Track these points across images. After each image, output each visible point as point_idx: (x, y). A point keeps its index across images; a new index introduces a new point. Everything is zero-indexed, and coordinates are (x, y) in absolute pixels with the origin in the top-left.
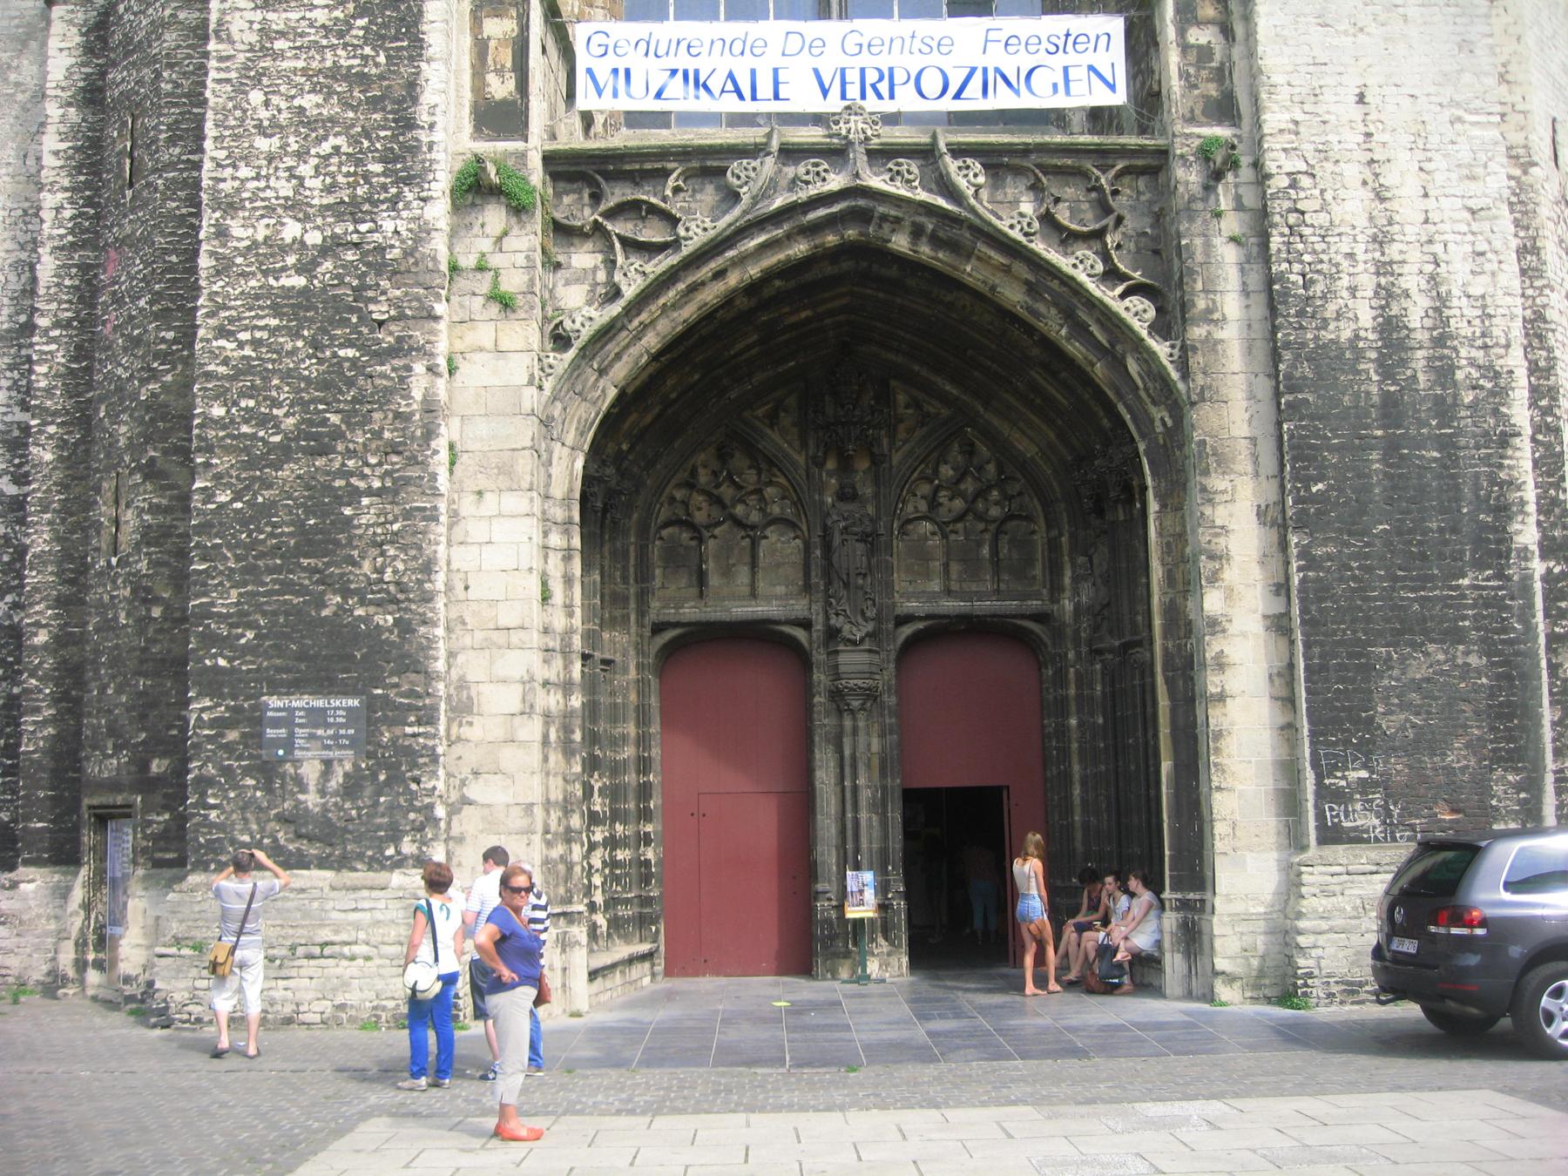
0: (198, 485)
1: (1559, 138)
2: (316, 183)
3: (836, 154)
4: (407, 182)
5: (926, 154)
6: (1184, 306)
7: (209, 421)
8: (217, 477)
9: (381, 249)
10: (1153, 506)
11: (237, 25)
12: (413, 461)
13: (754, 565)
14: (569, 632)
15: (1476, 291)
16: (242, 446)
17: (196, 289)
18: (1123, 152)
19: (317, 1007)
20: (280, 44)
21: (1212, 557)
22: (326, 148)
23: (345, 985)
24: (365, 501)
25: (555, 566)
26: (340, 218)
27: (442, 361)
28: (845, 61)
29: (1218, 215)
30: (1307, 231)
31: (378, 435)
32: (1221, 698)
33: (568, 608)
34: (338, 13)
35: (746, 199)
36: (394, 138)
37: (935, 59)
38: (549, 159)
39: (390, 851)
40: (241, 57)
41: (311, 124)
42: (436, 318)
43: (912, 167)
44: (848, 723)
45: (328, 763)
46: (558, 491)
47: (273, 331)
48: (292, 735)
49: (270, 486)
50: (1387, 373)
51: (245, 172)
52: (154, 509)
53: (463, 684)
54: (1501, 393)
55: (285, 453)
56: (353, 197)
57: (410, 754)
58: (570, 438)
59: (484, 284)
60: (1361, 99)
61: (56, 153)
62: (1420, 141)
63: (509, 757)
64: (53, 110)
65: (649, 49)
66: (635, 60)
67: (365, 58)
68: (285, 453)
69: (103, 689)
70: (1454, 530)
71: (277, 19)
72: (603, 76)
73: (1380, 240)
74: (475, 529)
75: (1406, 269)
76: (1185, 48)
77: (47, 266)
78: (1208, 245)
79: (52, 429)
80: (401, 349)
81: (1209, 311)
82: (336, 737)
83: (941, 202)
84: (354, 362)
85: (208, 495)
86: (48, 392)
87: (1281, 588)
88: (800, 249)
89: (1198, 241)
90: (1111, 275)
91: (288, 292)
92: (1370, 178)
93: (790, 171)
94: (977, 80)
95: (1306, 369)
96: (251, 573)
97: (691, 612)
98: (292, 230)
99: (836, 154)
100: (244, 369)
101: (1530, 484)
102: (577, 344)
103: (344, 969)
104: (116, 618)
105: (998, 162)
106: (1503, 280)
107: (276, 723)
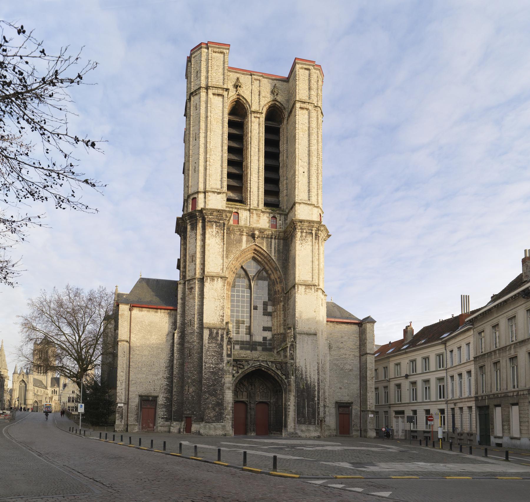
5: (266, 361)
7: (204, 383)
11: (206, 345)
17: (203, 370)
41: (213, 356)
54: (315, 387)
55: (211, 386)
57: (222, 413)
68: (211, 386)
69: (187, 405)
71: (210, 345)
73: (306, 373)
74: (227, 394)
80: (221, 377)
85: (204, 389)
87: (295, 402)
88: (254, 369)
98: (212, 366)
100: (207, 378)
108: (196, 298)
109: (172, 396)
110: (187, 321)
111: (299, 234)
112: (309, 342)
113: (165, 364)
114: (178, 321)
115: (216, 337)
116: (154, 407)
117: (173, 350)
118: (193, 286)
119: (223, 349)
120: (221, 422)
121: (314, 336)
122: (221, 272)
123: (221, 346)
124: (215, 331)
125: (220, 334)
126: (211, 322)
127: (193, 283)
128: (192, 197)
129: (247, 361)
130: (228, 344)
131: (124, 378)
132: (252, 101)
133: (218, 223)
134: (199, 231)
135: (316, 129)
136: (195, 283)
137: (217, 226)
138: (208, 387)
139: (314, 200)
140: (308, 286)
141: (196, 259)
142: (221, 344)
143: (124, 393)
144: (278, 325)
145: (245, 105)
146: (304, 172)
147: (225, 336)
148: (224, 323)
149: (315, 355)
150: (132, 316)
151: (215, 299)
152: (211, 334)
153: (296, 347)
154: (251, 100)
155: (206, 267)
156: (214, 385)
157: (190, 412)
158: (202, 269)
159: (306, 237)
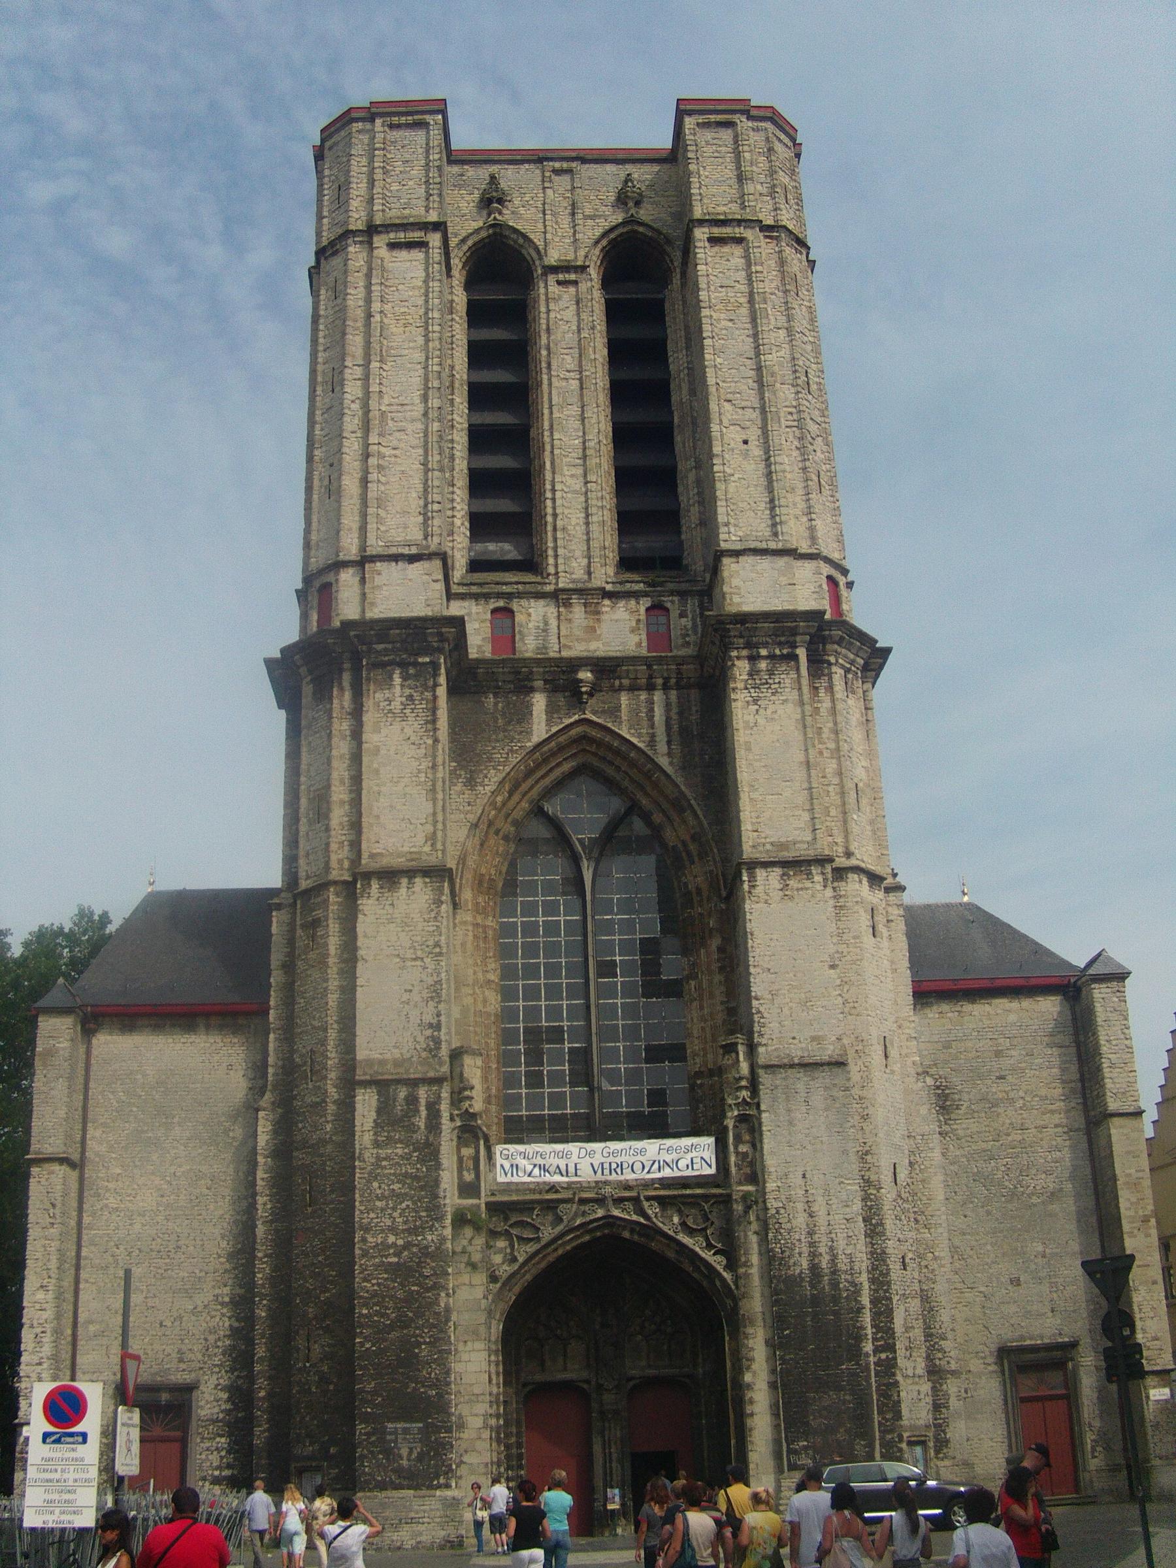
0: (358, 1340)
1: (897, 1171)
2: (400, 1220)
4: (436, 1219)
5: (636, 1200)
6: (737, 1260)
7: (361, 1315)
8: (365, 1337)
9: (427, 1247)
10: (727, 1338)
11: (367, 1155)
12: (441, 1331)
13: (565, 1356)
14: (498, 1394)
15: (848, 1252)
17: (355, 1263)
18: (714, 1196)
19: (410, 1543)
20: (384, 1163)
21: (748, 1360)
22: (404, 1205)
23: (421, 1534)
24: (423, 1347)
25: (493, 1369)
26: (410, 1234)
27: (451, 1291)
28: (603, 1160)
29: (750, 1223)
30: (782, 1231)
31: (427, 1321)
32: (752, 1415)
33: (498, 1385)
34: (406, 1150)
35: (565, 1221)
36: (429, 1202)
37: (639, 1158)
38: (487, 1204)
39: (435, 1482)
40: (369, 1168)
41: (398, 1196)
42: (449, 1274)
43: (629, 1205)
44: (607, 1425)
45: (411, 1449)
46: (493, 1339)
47: (386, 1279)
48: (397, 1438)
49: (386, 1341)
50: (813, 1286)
51: (372, 1215)
52: (329, 1345)
53: (460, 1417)
54: (857, 1292)
55: (391, 1328)
56: (415, 1226)
58: (497, 1317)
59: (465, 1259)
60: (804, 1176)
61: (263, 1179)
62: (827, 1192)
63: (479, 1445)
64: (261, 1159)
65: (525, 1156)
66: (523, 1163)
67: (417, 1169)
68: (391, 1328)
70: (840, 1347)
71: (383, 1153)
72: (507, 1166)
73: (811, 1233)
74: (465, 1357)
75: (821, 1244)
76: (737, 1153)
77: (260, 1230)
78: (746, 1236)
79: (265, 1302)
80: (436, 1287)
81: (746, 1262)
82: (414, 1438)
83: (642, 1220)
84: (418, 1292)
86: (263, 1285)
87: (773, 1371)
88: (587, 1238)
89: (742, 1234)
90: (709, 1246)
91: (390, 1264)
92: (806, 1207)
93: (582, 1208)
94: (656, 1165)
95: (782, 1286)
97: (538, 1378)
98: (391, 1239)
99: (600, 1201)
100: (375, 1294)
101: (869, 1327)
102: (501, 1281)
103: (421, 1528)
104: (310, 1388)
105: (663, 1202)
106: (858, 1247)
107: (391, 1434)
108: (331, 961)
109: (251, 1378)
110: (302, 1056)
111: (741, 669)
112: (818, 1099)
113: (224, 1244)
115: (406, 1115)
116: (178, 1434)
118: (319, 913)
119: (438, 1166)
120: (439, 1487)
121: (835, 1070)
122: (427, 849)
123: (429, 1153)
124: (402, 1093)
125: (423, 1102)
126: (388, 1056)
129: (550, 1206)
130: (461, 1142)
131: (49, 1314)
132: (549, 236)
134: (342, 700)
136: (327, 901)
139: (794, 533)
140: (795, 866)
141: (329, 810)
142: (428, 1144)
145: (524, 252)
146: (746, 442)
147: (444, 1107)
148: (444, 1052)
149: (845, 1152)
151: (404, 960)
153: (760, 1124)
154: (545, 233)
155: (364, 837)
156: (402, 1323)
157: (316, 1446)
159: (771, 673)
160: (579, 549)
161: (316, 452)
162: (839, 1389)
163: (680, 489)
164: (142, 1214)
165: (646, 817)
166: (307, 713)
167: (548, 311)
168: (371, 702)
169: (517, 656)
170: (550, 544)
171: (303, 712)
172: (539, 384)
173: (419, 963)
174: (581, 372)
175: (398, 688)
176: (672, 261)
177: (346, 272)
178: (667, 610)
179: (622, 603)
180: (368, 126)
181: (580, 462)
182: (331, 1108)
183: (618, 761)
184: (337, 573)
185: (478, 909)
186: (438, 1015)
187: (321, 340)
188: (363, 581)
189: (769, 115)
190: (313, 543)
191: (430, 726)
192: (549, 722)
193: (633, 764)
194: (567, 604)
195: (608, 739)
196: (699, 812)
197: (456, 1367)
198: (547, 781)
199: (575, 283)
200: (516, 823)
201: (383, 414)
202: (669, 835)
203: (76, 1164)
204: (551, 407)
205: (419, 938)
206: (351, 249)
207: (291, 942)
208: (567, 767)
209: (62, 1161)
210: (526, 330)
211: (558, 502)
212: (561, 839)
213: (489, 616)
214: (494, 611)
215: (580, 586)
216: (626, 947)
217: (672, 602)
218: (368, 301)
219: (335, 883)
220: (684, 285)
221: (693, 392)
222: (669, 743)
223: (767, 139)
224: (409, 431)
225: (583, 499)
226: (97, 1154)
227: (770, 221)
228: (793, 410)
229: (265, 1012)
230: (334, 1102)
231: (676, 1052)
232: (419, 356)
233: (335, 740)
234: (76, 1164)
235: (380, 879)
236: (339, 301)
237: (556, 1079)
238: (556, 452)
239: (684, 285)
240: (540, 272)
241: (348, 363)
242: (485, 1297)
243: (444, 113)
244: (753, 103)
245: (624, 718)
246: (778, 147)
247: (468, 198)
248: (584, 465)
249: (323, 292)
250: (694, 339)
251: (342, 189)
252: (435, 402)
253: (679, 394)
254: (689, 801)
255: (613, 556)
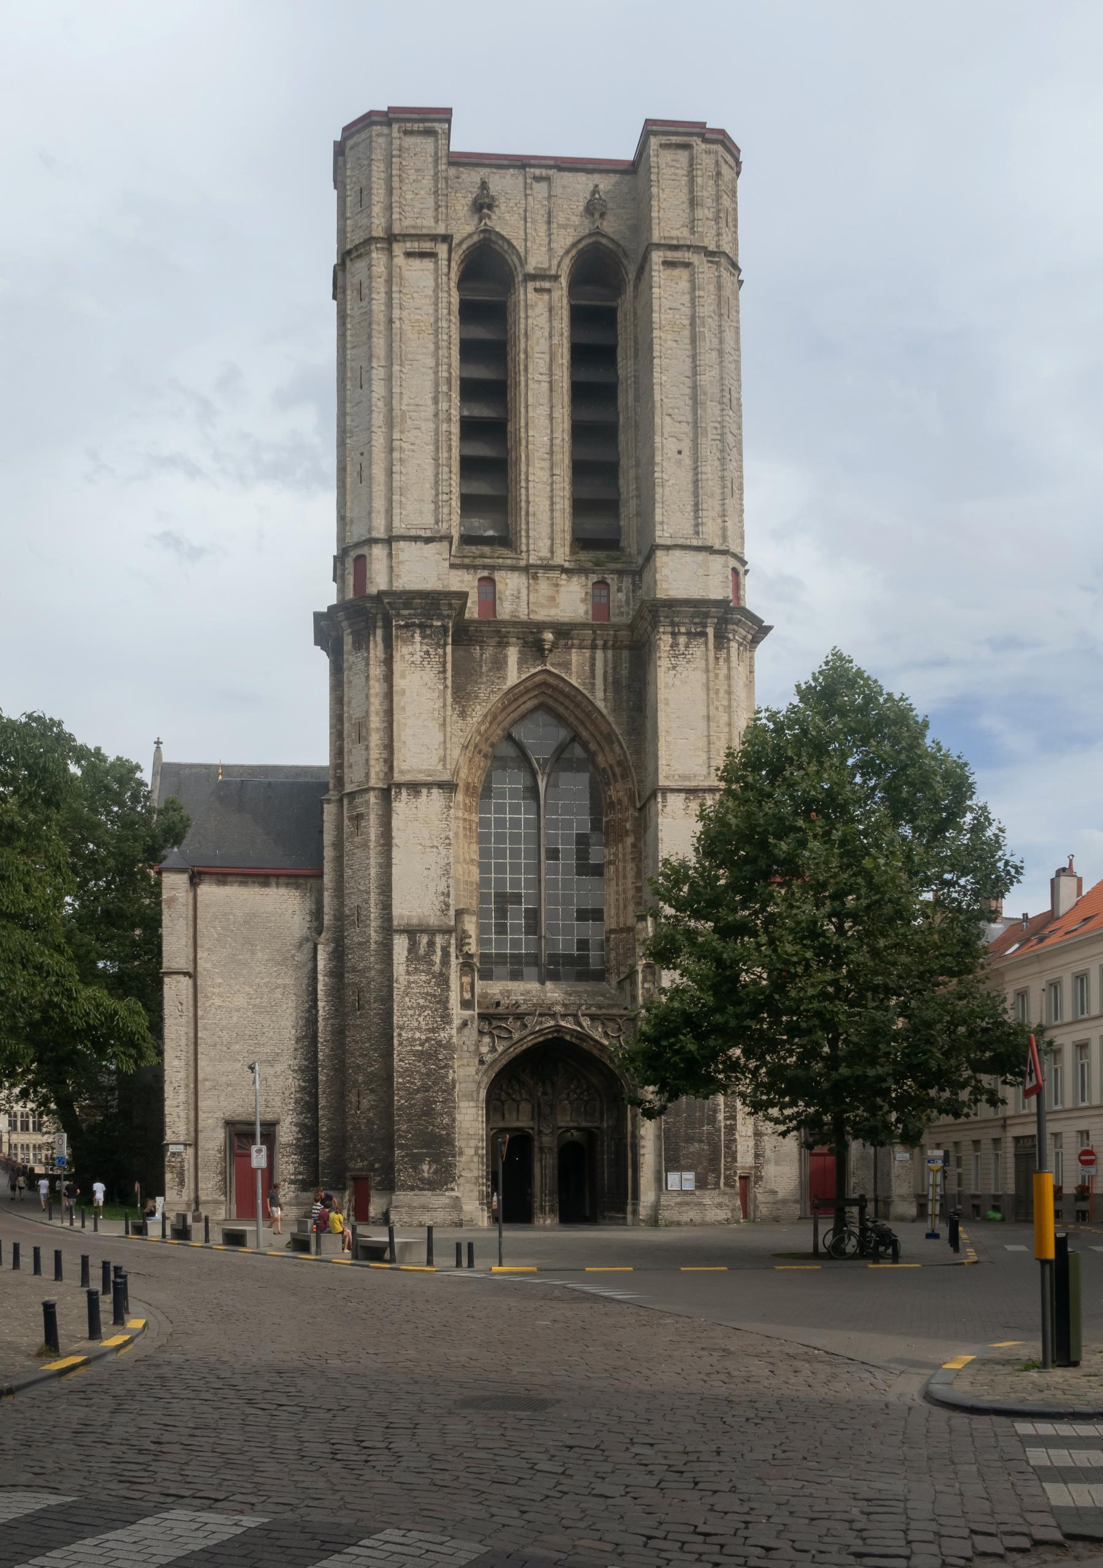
3: (553, 1016)
7: (398, 1083)
11: (401, 979)
12: (449, 1094)
16: (407, 1089)
17: (393, 1049)
55: (418, 1091)
68: (418, 1091)
71: (412, 979)
74: (464, 1111)
76: (643, 988)
80: (446, 1066)
85: (399, 1101)
88: (541, 1039)
96: (410, 1121)
98: (417, 1035)
100: (407, 1070)
105: (593, 1018)
108: (372, 845)
110: (351, 909)
114: (326, 909)
117: (314, 992)
118: (362, 810)
119: (448, 988)
122: (440, 767)
123: (443, 980)
124: (424, 940)
126: (414, 913)
127: (361, 803)
128: (353, 554)
129: (519, 1017)
130: (463, 973)
133: (427, 626)
134: (377, 650)
135: (716, 318)
136: (367, 802)
137: (423, 637)
138: (410, 1093)
142: (441, 974)
143: (183, 1114)
144: (621, 902)
145: (507, 257)
148: (452, 912)
150: (199, 899)
152: (413, 948)
155: (395, 757)
158: (385, 761)
160: (545, 530)
161: (348, 441)
162: (701, 1141)
163: (621, 482)
164: (238, 1010)
165: (585, 746)
166: (351, 658)
167: (527, 317)
168: (398, 655)
169: (499, 618)
170: (524, 526)
171: (345, 656)
172: (517, 384)
173: (435, 850)
174: (551, 376)
175: (418, 644)
176: (627, 273)
177: (370, 277)
178: (608, 585)
179: (575, 579)
180: (385, 130)
181: (547, 456)
182: (373, 946)
183: (567, 702)
184: (371, 547)
185: (467, 809)
186: (448, 887)
187: (349, 338)
188: (390, 555)
189: (721, 137)
190: (348, 519)
191: (441, 676)
192: (520, 670)
193: (578, 705)
194: (535, 577)
195: (561, 685)
196: (624, 744)
197: (458, 1117)
198: (516, 715)
199: (549, 291)
200: (492, 745)
201: (403, 412)
202: (600, 759)
203: (192, 975)
204: (527, 407)
205: (434, 832)
206: (374, 255)
207: (339, 828)
208: (530, 704)
209: (186, 974)
210: (506, 331)
211: (531, 491)
212: (523, 757)
213: (476, 583)
214: (480, 580)
215: (545, 562)
216: (566, 840)
217: (613, 579)
218: (389, 305)
219: (374, 789)
220: (635, 297)
221: (637, 399)
222: (605, 691)
223: (717, 162)
224: (423, 429)
225: (548, 489)
226: (205, 969)
227: (712, 247)
228: (718, 425)
229: (320, 876)
230: (376, 943)
231: (596, 915)
232: (430, 362)
233: (372, 683)
234: (192, 975)
235: (408, 789)
236: (364, 304)
237: (515, 929)
238: (530, 447)
239: (635, 297)
240: (520, 278)
241: (374, 365)
242: (477, 1074)
243: (449, 121)
244: (708, 126)
245: (574, 670)
246: (725, 170)
247: (463, 201)
248: (551, 459)
249: (349, 292)
250: (644, 351)
251: (364, 193)
252: (443, 406)
253: (625, 398)
254: (617, 736)
255: (568, 537)
